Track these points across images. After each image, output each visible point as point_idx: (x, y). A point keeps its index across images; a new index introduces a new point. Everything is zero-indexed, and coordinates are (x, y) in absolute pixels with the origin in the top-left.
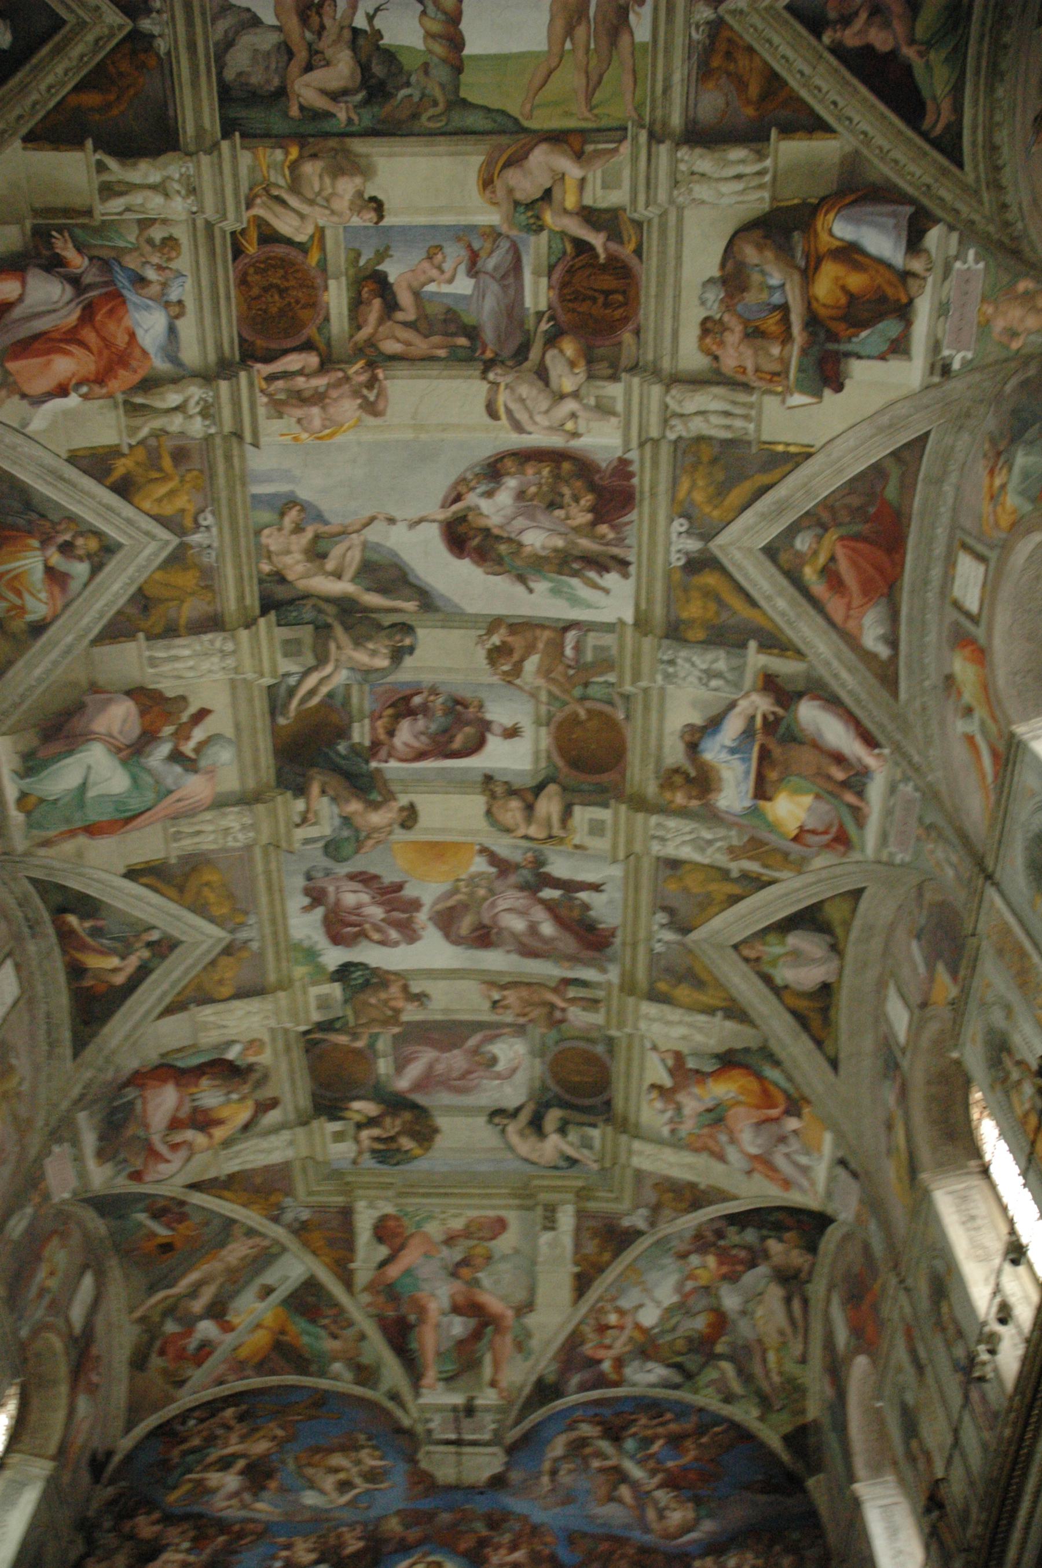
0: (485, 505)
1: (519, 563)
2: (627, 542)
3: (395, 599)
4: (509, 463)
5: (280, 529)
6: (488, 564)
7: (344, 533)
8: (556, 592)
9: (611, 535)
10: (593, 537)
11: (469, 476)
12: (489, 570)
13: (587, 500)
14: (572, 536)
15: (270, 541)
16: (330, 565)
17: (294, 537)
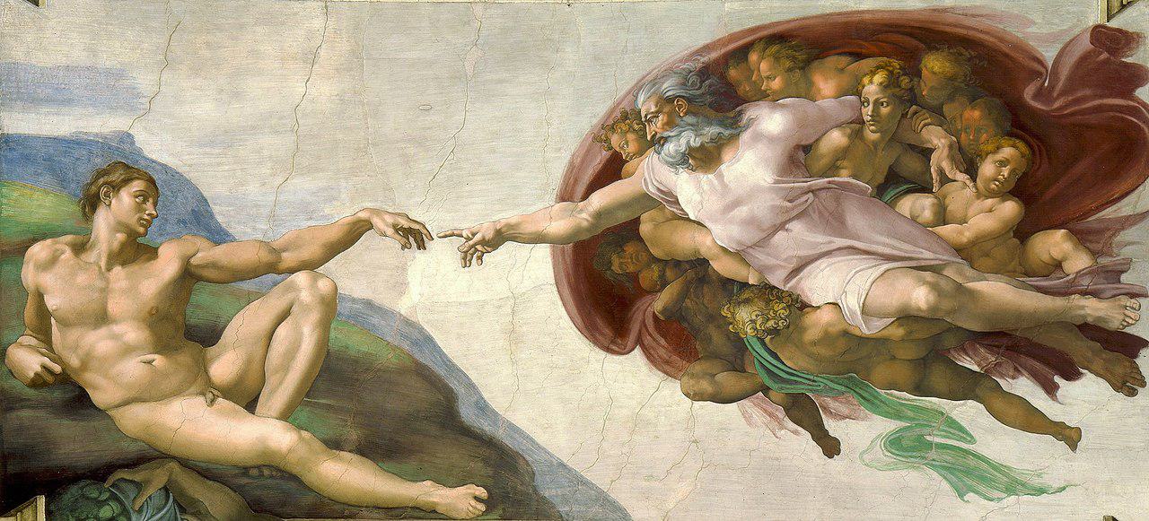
0: (690, 190)
1: (792, 359)
2: (1124, 278)
3: (416, 478)
4: (762, 64)
5: (80, 248)
6: (697, 367)
7: (272, 268)
8: (908, 447)
9: (1078, 262)
10: (1023, 271)
11: (646, 105)
12: (705, 386)
13: (1004, 158)
14: (957, 272)
15: (48, 280)
16: (224, 365)
17: (117, 269)
